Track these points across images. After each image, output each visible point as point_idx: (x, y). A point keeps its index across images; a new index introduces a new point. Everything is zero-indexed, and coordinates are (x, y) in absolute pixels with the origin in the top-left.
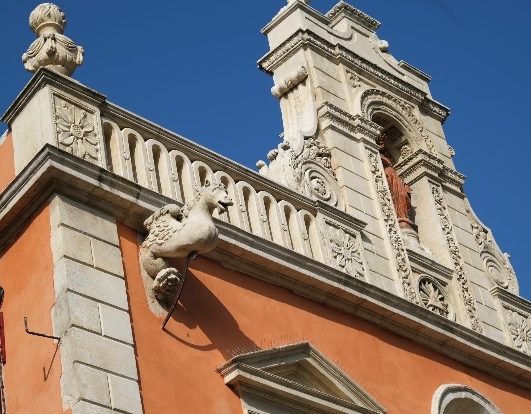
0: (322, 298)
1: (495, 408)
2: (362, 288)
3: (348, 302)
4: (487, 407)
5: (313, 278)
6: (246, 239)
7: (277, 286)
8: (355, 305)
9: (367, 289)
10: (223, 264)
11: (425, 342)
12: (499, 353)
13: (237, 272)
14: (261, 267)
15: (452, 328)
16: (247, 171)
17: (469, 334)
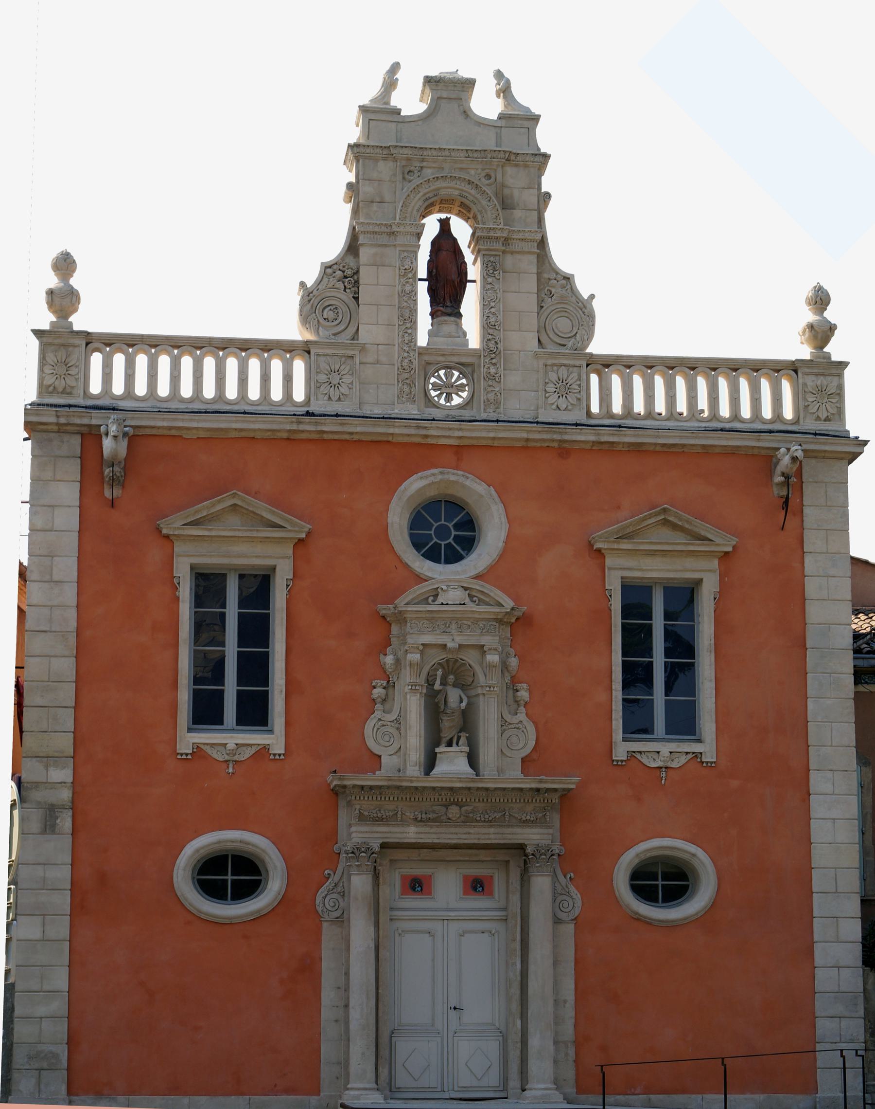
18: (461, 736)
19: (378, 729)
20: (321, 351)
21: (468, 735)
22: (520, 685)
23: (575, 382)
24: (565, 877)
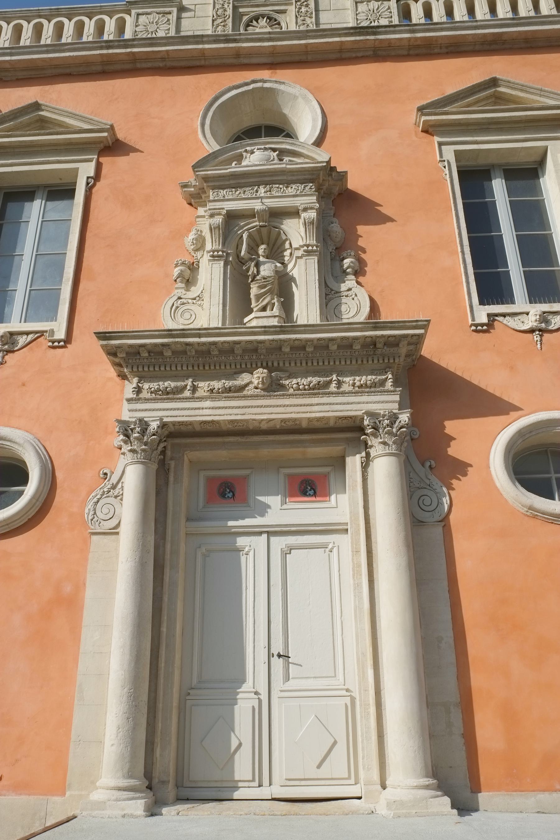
0: (99, 68)
1: (291, 85)
2: (124, 44)
3: (124, 61)
4: (282, 87)
5: (73, 56)
6: (4, 52)
7: (56, 75)
8: (132, 61)
9: (130, 43)
10: (4, 78)
11: (218, 62)
12: (300, 39)
13: (17, 80)
14: (34, 68)
15: (234, 39)
16: (58, 9)
17: (256, 36)
18: (274, 303)
19: (177, 307)
20: (140, 11)
21: (282, 300)
23: (386, 10)
24: (423, 465)
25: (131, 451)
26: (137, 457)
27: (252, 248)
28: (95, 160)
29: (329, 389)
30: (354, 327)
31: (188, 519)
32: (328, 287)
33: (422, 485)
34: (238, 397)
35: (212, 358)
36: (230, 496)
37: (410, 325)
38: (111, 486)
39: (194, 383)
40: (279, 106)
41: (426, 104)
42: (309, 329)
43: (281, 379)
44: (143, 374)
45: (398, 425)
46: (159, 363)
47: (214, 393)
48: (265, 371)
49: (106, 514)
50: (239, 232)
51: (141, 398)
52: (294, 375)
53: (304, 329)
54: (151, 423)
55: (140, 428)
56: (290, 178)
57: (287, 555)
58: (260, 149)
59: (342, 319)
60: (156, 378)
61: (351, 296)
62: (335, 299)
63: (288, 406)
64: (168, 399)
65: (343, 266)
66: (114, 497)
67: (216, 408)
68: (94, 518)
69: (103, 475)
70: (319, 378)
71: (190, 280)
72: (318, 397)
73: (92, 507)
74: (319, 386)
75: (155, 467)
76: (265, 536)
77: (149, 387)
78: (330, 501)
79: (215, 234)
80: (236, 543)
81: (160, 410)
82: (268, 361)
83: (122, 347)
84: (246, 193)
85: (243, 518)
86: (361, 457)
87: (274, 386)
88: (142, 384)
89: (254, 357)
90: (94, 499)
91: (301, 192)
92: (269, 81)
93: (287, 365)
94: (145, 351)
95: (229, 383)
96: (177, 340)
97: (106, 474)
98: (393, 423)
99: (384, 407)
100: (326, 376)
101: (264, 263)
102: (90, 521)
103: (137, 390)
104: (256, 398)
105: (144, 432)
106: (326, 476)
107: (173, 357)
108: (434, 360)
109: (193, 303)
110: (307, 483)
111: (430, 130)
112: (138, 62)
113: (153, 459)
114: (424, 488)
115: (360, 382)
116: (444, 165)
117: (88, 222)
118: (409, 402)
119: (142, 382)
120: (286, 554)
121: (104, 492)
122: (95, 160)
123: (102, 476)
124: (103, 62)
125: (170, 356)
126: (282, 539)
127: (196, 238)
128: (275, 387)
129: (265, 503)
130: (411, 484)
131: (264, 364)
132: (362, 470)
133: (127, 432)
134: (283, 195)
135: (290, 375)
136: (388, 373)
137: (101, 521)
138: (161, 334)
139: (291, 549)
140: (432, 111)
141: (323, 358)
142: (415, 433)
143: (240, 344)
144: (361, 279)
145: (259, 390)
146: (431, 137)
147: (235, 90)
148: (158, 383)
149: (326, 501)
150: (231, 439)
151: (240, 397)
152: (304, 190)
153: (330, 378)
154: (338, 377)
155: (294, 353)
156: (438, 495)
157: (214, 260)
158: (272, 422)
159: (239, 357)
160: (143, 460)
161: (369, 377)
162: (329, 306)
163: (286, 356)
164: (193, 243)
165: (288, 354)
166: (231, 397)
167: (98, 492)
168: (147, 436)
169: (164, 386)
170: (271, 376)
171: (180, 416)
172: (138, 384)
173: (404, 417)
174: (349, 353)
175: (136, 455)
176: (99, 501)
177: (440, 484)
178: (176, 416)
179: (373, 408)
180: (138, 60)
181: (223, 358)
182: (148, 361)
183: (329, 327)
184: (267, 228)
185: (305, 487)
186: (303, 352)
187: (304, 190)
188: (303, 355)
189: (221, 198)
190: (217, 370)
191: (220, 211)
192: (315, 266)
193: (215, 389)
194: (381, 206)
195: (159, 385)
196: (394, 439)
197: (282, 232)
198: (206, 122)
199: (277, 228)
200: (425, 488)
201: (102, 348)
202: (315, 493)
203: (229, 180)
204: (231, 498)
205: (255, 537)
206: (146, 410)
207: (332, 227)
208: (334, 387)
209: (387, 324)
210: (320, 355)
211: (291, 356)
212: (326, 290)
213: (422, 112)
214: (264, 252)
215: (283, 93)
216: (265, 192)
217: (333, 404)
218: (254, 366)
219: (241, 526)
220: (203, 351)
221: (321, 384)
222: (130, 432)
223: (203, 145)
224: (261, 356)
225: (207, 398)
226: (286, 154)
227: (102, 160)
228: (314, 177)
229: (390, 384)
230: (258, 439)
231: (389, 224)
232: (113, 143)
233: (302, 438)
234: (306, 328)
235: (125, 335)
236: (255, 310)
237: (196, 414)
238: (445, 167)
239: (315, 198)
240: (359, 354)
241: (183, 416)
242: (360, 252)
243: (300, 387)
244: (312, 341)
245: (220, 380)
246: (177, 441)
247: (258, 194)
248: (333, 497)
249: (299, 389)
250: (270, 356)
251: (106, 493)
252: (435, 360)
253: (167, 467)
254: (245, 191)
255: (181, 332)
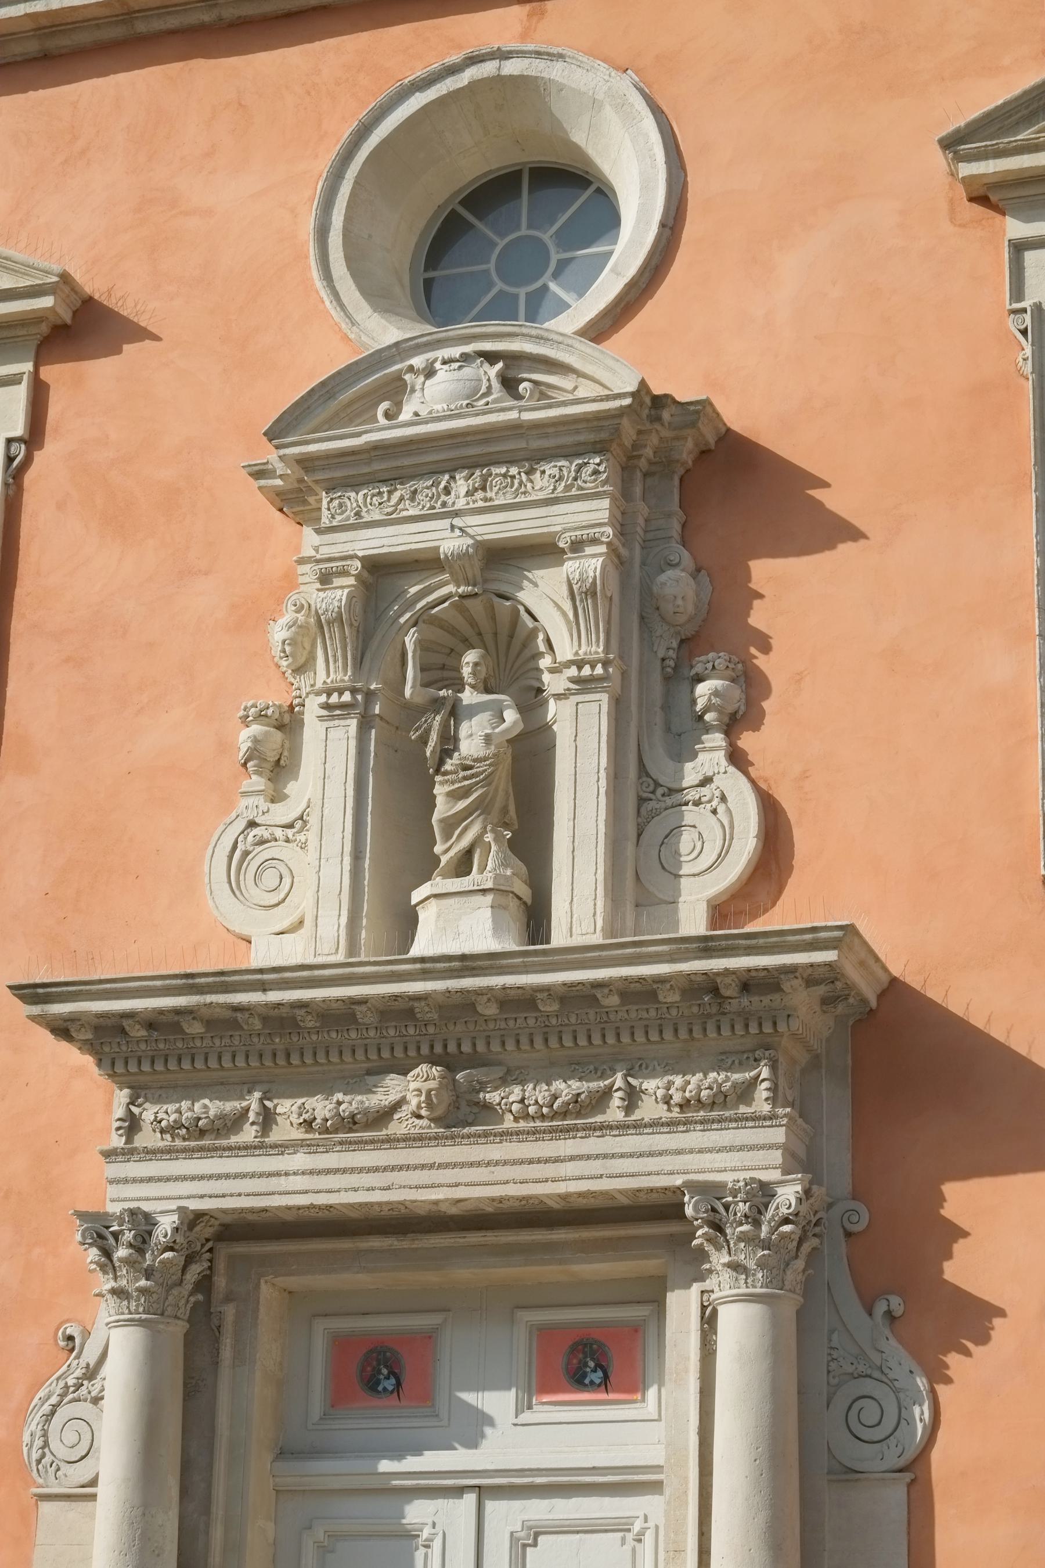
0: (32, 47)
1: (582, 62)
19: (246, 853)
22: (703, 658)
25: (114, 1292)
26: (128, 1307)
27: (452, 650)
28: (25, 377)
29: (604, 1113)
30: (651, 952)
31: (284, 1453)
32: (648, 775)
33: (862, 1368)
34: (372, 1142)
35: (306, 1035)
36: (390, 1388)
37: (797, 941)
38: (84, 1371)
39: (267, 1103)
40: (557, 124)
41: (968, 125)
42: (533, 961)
43: (482, 1087)
44: (142, 1078)
45: (773, 1216)
46: (179, 1052)
47: (316, 1130)
48: (436, 1071)
49: (72, 1447)
50: (402, 620)
51: (136, 1149)
52: (517, 1073)
53: (523, 962)
54: (161, 1219)
55: (133, 1232)
56: (536, 444)
57: (528, 1549)
58: (451, 361)
59: (681, 876)
60: (174, 1087)
61: (710, 801)
62: (664, 814)
63: (497, 1163)
64: (201, 1149)
65: (694, 702)
66: (91, 1402)
67: (320, 1172)
68: (43, 1456)
69: (63, 1341)
70: (578, 1084)
71: (282, 762)
72: (574, 1138)
73: (40, 1427)
74: (579, 1107)
75: (180, 1328)
76: (471, 1498)
77: (156, 1117)
78: (643, 1400)
79: (331, 638)
80: (404, 1518)
81: (184, 1178)
82: (446, 1040)
83: (79, 1020)
84: (419, 497)
85: (417, 1450)
86: (702, 1292)
87: (465, 1109)
88: (139, 1106)
89: (411, 1031)
90: (42, 1405)
91: (568, 488)
92: (518, 52)
93: (496, 1047)
94: (137, 1027)
95: (352, 1103)
96: (210, 998)
97: (71, 1338)
98: (762, 1209)
99: (745, 1163)
100: (599, 1074)
101: (474, 710)
102: (34, 1464)
103: (127, 1124)
104: (419, 1144)
105: (144, 1242)
106: (636, 1331)
107: (209, 1035)
108: (930, 994)
109: (287, 841)
110: (587, 1349)
111: (994, 198)
112: (137, 17)
113: (169, 1311)
114: (867, 1376)
115: (685, 1092)
116: (1022, 327)
117: (15, 586)
118: (848, 1123)
119: (140, 1100)
120: (525, 1546)
121: (67, 1387)
122: (25, 377)
123: (62, 1344)
124: (39, 29)
125: (201, 1033)
126: (517, 1505)
127: (291, 639)
128: (468, 1109)
129: (477, 1408)
130: (831, 1364)
131: (438, 1049)
132: (702, 1325)
133: (105, 1242)
134: (517, 500)
135: (509, 1072)
136: (762, 1064)
137: (62, 1465)
138: (167, 985)
139: (536, 1533)
140: (986, 146)
141: (588, 1027)
142: (855, 1219)
143: (366, 1002)
144: (747, 741)
145: (425, 1122)
146: (998, 217)
147: (417, 94)
148: (178, 1105)
149: (634, 1402)
150: (376, 1242)
151: (378, 1141)
152: (575, 479)
153: (607, 1082)
154: (629, 1079)
155: (510, 1018)
156: (901, 1395)
157: (332, 718)
158: (462, 1204)
159: (372, 1033)
160: (144, 1316)
161: (713, 1075)
162: (645, 836)
163: (491, 1026)
164: (284, 651)
165: (495, 1020)
166: (356, 1143)
167: (51, 1388)
168: (153, 1252)
169: (189, 1114)
170: (454, 1080)
171: (232, 1195)
172: (130, 1106)
173: (788, 1195)
174: (653, 1013)
175: (125, 1303)
176: (56, 1411)
177: (909, 1363)
178: (224, 1196)
179: (717, 1165)
180: (139, 11)
181: (334, 1035)
182: (149, 1048)
183: (586, 955)
184: (480, 598)
185: (580, 1362)
186: (535, 1015)
187: (575, 479)
188: (534, 1021)
189: (351, 522)
190: (322, 1065)
191: (344, 563)
192: (602, 723)
193: (317, 1121)
194: (825, 485)
195: (179, 1111)
196: (760, 1253)
197: (521, 609)
198: (334, 218)
199: (507, 599)
200: (870, 1377)
201: (33, 1021)
202: (606, 1377)
203: (369, 462)
204: (392, 1392)
205: (446, 1500)
206: (150, 1180)
207: (664, 584)
208: (619, 1107)
209: (737, 942)
210: (579, 1022)
211: (503, 1025)
212: (642, 784)
213: (955, 152)
214: (474, 673)
215: (562, 90)
216: (469, 494)
217: (613, 1156)
218: (412, 1053)
219: (409, 1473)
220: (282, 1018)
221: (582, 1101)
222: (112, 1240)
223: (323, 302)
224: (428, 1028)
225: (297, 1145)
226: (526, 364)
227: (47, 373)
228: (603, 435)
229: (765, 1094)
230: (442, 1241)
231: (846, 549)
232: (75, 313)
233: (554, 1237)
234: (525, 960)
235: (82, 990)
236: (444, 859)
237: (271, 1189)
238: (1024, 332)
239: (606, 503)
240: (680, 1013)
241: (240, 1195)
242: (753, 650)
243: (530, 1108)
244: (549, 990)
245: (329, 1093)
246: (241, 1248)
247: (450, 499)
248: (652, 1393)
249: (526, 1116)
250: (451, 1027)
251: (72, 1389)
252: (934, 994)
253: (215, 1321)
254: (415, 492)
255: (217, 979)
